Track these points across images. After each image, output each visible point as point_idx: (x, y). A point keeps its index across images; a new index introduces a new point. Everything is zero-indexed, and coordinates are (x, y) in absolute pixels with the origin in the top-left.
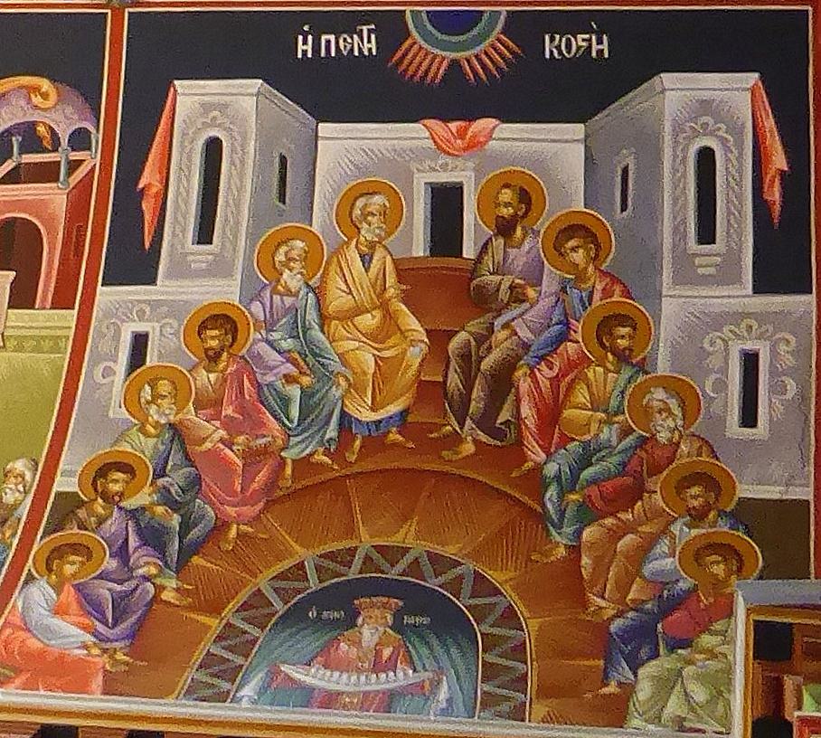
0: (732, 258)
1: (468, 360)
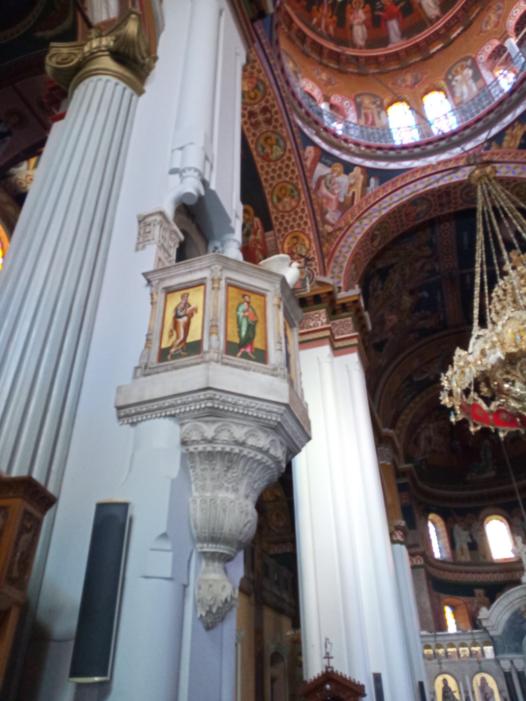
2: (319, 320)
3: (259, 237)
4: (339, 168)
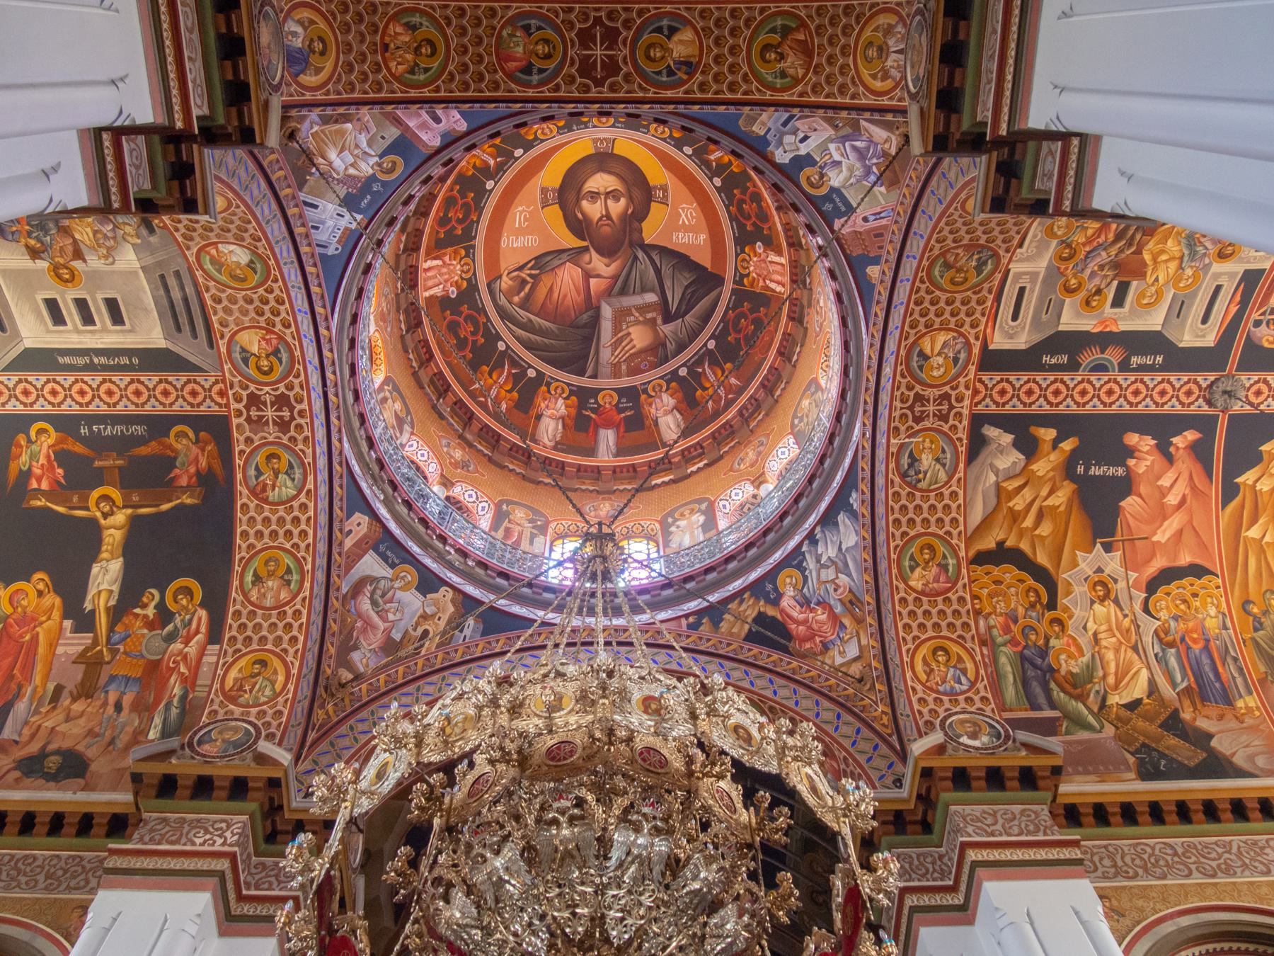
0: (1014, 282)
1: (1130, 244)
2: (220, 836)
3: (192, 650)
4: (410, 575)
